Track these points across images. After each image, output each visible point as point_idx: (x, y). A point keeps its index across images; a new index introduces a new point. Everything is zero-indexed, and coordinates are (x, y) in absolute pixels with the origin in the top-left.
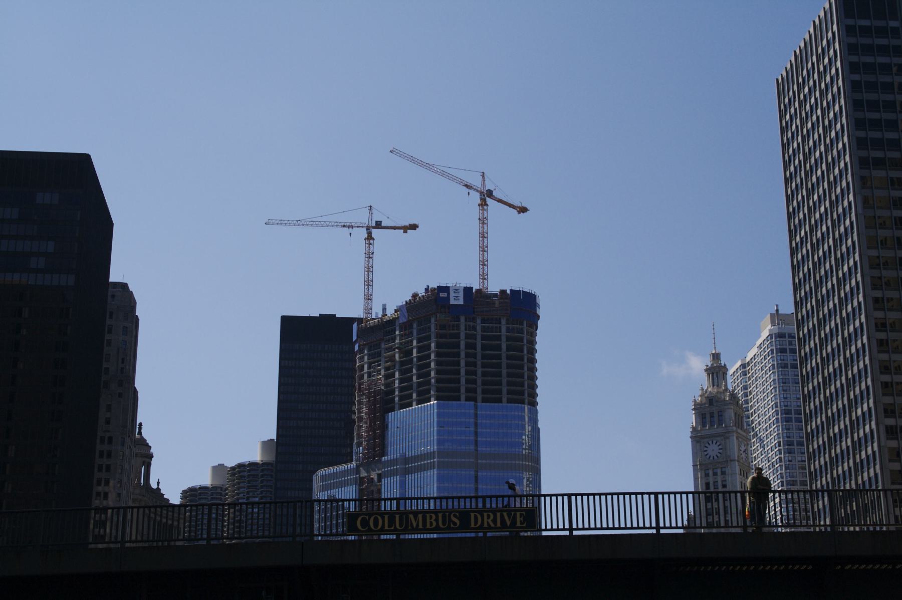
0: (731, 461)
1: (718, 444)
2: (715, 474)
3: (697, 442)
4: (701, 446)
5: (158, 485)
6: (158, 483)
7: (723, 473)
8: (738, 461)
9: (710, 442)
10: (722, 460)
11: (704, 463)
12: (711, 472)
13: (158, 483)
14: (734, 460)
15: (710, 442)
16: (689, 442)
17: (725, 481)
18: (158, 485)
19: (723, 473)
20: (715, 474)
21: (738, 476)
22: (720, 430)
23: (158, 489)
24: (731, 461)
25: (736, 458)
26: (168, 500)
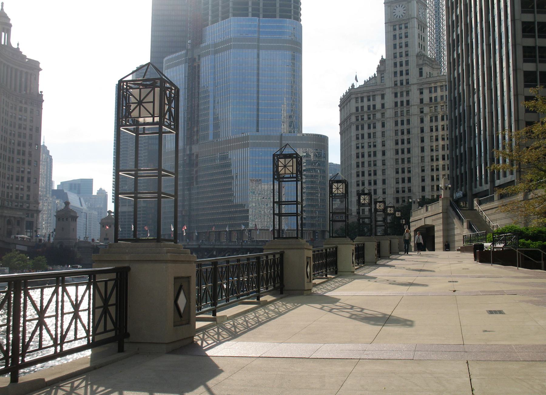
0: (412, 18)
1: (403, 6)
2: (400, 28)
3: (389, 6)
4: (391, 9)
5: (18, 45)
6: (18, 44)
7: (406, 27)
8: (417, 18)
9: (398, 6)
10: (405, 18)
11: (392, 21)
12: (397, 27)
13: (18, 44)
14: (414, 18)
15: (398, 6)
16: (383, 6)
17: (407, 33)
18: (18, 45)
19: (406, 27)
20: (400, 28)
21: (416, 29)
23: (18, 48)
24: (412, 18)
25: (416, 16)
26: (21, 52)
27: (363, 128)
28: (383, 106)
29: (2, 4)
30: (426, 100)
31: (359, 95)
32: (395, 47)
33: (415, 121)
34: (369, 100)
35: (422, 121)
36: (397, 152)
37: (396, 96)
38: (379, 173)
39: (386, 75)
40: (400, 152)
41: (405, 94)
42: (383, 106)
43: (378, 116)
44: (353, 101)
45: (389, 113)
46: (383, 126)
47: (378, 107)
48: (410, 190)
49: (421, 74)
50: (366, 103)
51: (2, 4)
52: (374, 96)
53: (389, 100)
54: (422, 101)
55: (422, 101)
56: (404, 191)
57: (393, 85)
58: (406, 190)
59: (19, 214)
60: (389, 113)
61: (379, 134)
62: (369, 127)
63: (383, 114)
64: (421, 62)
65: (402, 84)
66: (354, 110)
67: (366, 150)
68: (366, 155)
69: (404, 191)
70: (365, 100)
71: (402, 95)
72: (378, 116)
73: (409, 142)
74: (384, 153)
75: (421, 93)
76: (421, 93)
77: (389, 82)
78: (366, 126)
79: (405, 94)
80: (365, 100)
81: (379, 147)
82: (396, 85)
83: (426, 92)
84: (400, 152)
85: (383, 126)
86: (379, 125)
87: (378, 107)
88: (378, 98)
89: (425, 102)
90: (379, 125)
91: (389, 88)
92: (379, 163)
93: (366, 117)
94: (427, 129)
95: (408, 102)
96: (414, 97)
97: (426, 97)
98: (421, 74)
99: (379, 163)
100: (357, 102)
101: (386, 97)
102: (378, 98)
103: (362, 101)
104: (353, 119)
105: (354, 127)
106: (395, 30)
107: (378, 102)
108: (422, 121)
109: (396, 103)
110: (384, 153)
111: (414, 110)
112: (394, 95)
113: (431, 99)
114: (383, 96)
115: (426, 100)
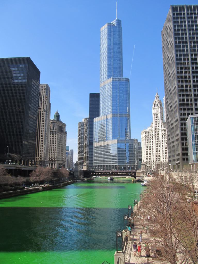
23: (61, 121)
29: (57, 110)
30: (163, 134)
35: (162, 139)
43: (151, 137)
44: (145, 133)
45: (154, 137)
47: (151, 135)
49: (162, 127)
51: (57, 110)
52: (150, 132)
53: (154, 133)
54: (162, 134)
59: (61, 162)
60: (154, 137)
61: (151, 142)
62: (149, 140)
65: (157, 129)
66: (145, 136)
70: (148, 133)
72: (151, 137)
82: (155, 129)
83: (163, 131)
87: (151, 135)
88: (151, 133)
89: (163, 134)
94: (164, 141)
95: (159, 134)
96: (160, 133)
97: (163, 132)
98: (162, 127)
102: (151, 133)
104: (145, 138)
105: (145, 140)
107: (151, 134)
108: (162, 139)
109: (156, 135)
114: (152, 132)
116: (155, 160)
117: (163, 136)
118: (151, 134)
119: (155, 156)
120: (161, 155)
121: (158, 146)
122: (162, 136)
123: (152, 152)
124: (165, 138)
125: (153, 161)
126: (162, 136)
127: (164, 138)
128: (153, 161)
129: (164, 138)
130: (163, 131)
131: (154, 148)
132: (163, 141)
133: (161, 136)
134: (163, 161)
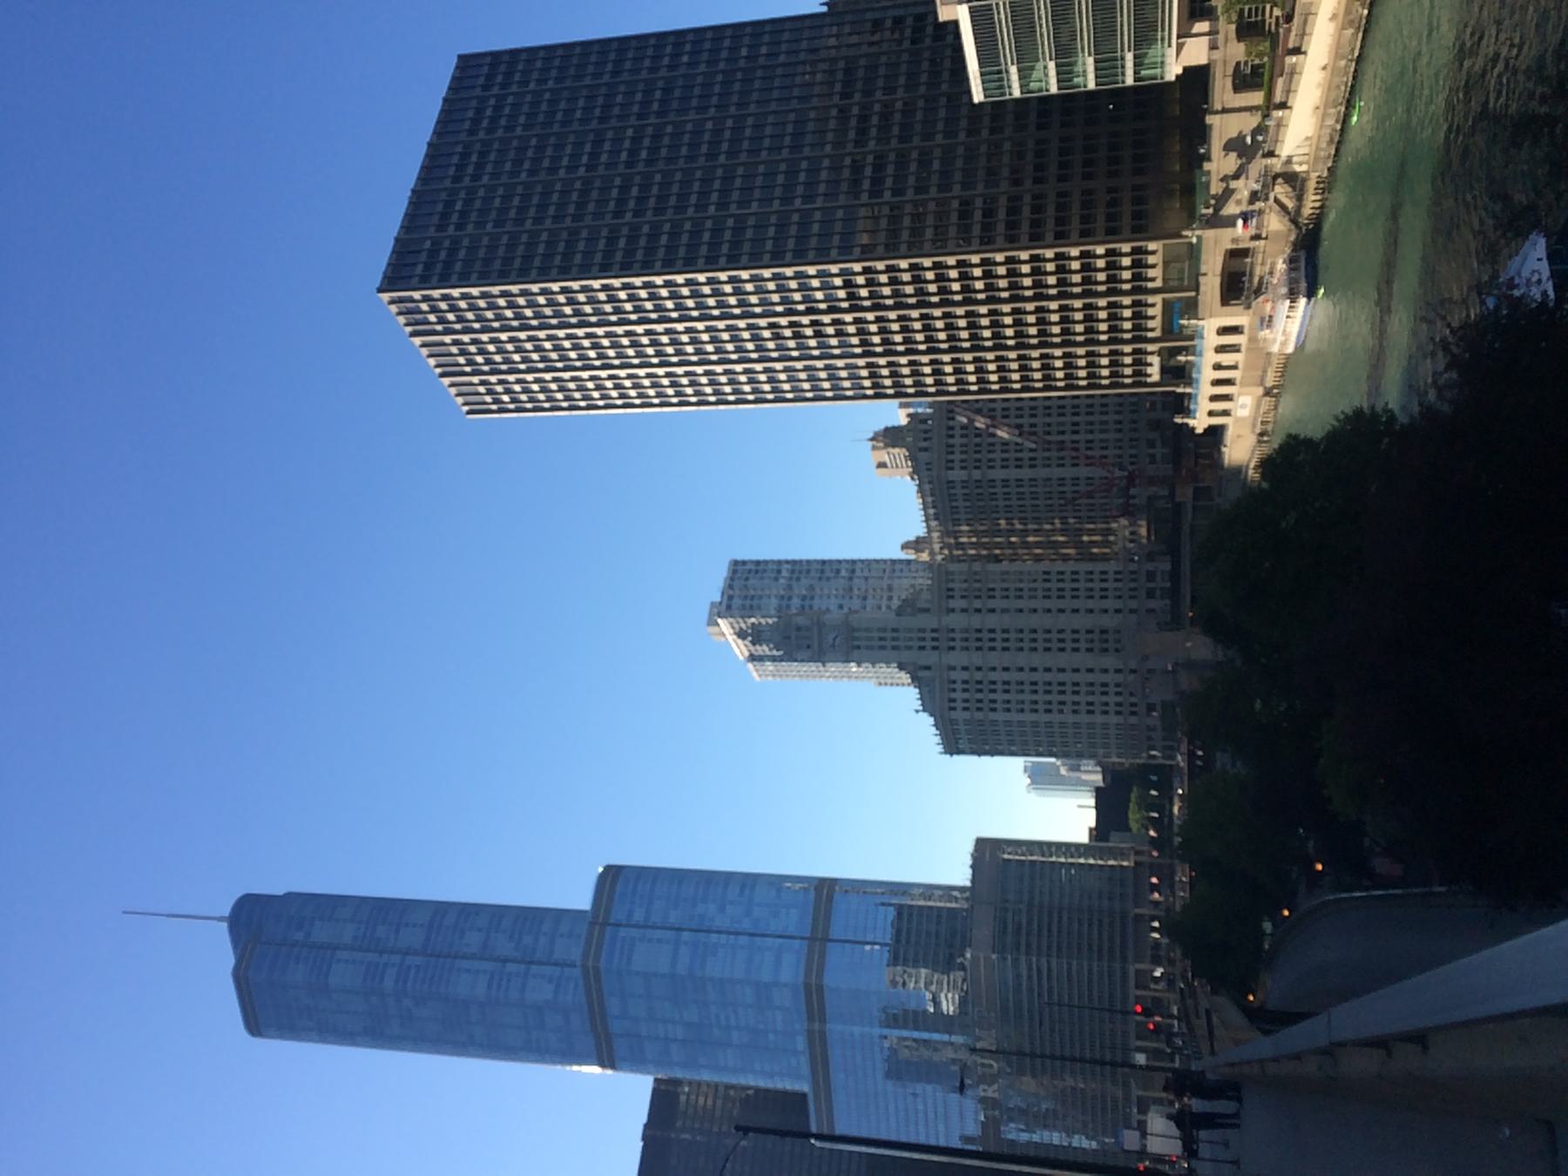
3: (825, 654)
20: (857, 639)
22: (815, 630)
27: (994, 701)
28: (965, 669)
30: (963, 603)
31: (946, 705)
32: (883, 648)
33: (992, 621)
34: (954, 690)
35: (993, 611)
36: (1035, 649)
37: (953, 648)
38: (1062, 677)
39: (923, 662)
40: (1033, 645)
41: (952, 635)
42: (965, 669)
43: (978, 676)
46: (994, 669)
47: (965, 675)
48: (1089, 632)
49: (927, 610)
50: (958, 695)
54: (964, 610)
55: (964, 610)
56: (1092, 641)
57: (937, 652)
58: (1090, 636)
61: (1006, 676)
63: (979, 669)
64: (909, 610)
66: (967, 715)
67: (1027, 697)
68: (1035, 697)
69: (1092, 641)
70: (953, 695)
71: (953, 640)
72: (978, 676)
73: (1021, 631)
74: (1034, 670)
75: (953, 610)
76: (953, 610)
77: (930, 658)
78: (992, 696)
79: (952, 635)
80: (953, 695)
81: (1026, 676)
84: (1033, 645)
85: (994, 669)
86: (993, 676)
87: (965, 675)
88: (954, 675)
90: (993, 676)
91: (940, 657)
92: (1048, 677)
93: (979, 696)
96: (956, 621)
97: (958, 603)
98: (927, 610)
99: (1048, 677)
100: (954, 709)
101: (953, 663)
102: (954, 675)
103: (954, 701)
104: (979, 715)
105: (992, 716)
106: (858, 647)
108: (993, 611)
110: (1034, 670)
111: (976, 621)
112: (951, 652)
113: (963, 597)
114: (953, 668)
115: (963, 603)
116: (1110, 661)
117: (977, 604)
118: (958, 675)
119: (1090, 660)
120: (1081, 621)
121: (1034, 640)
122: (978, 611)
123: (1062, 677)
124: (990, 597)
125: (1118, 671)
126: (978, 611)
127: (991, 604)
128: (1118, 671)
129: (991, 604)
130: (952, 604)
131: (1037, 660)
132: (1005, 611)
133: (976, 621)
134: (1120, 616)
